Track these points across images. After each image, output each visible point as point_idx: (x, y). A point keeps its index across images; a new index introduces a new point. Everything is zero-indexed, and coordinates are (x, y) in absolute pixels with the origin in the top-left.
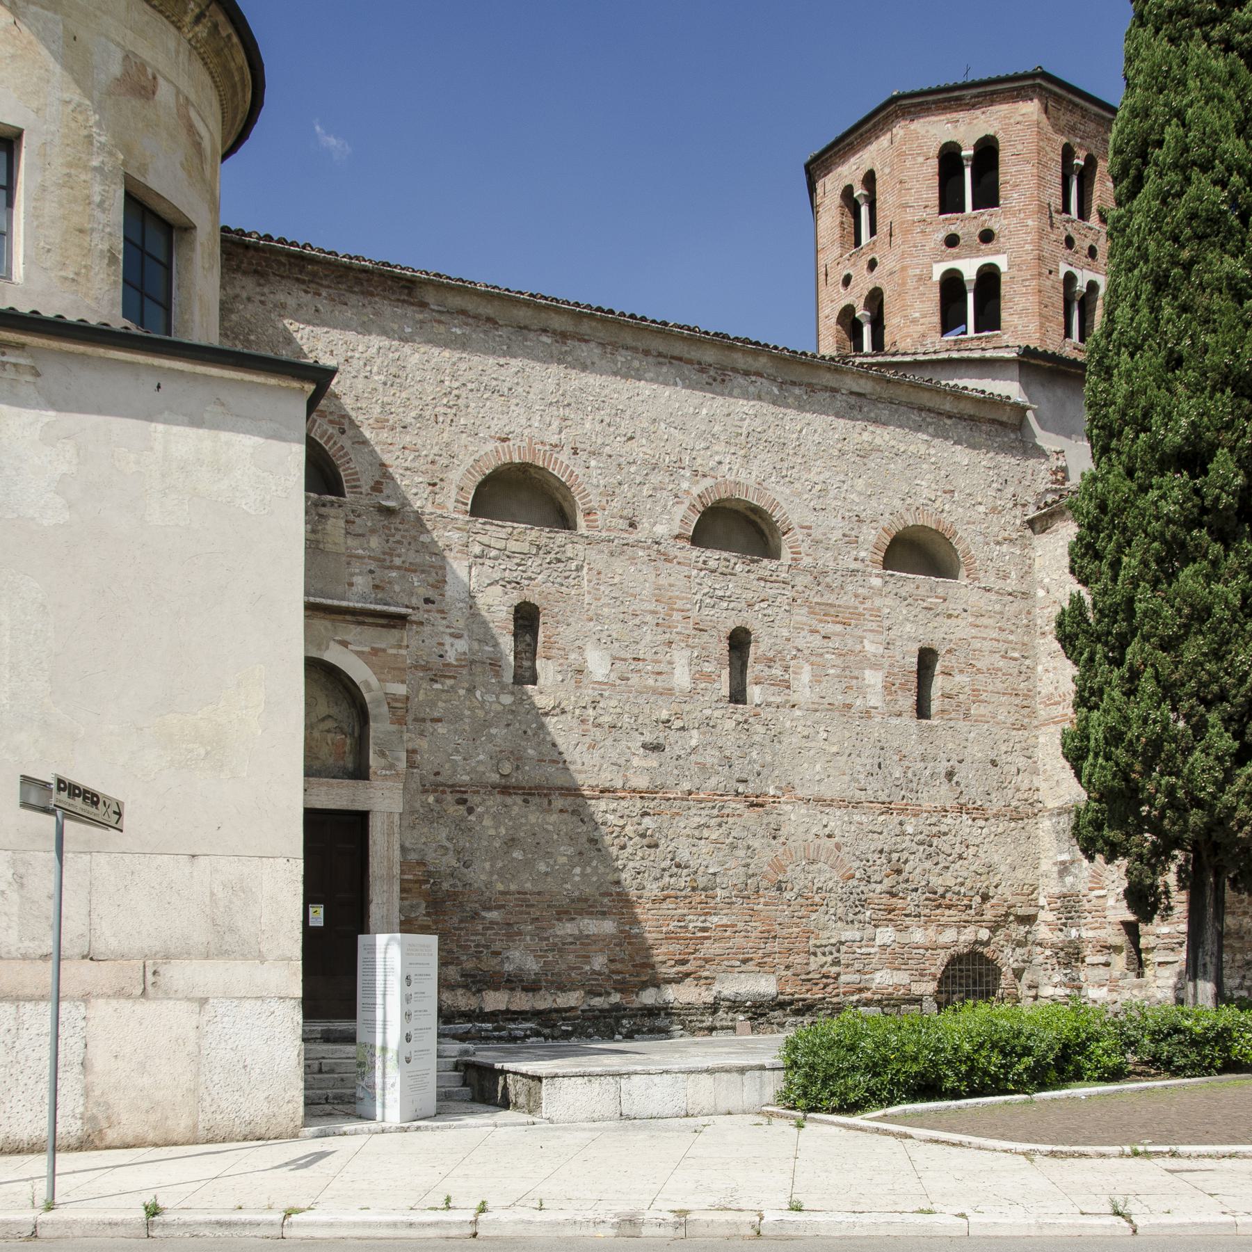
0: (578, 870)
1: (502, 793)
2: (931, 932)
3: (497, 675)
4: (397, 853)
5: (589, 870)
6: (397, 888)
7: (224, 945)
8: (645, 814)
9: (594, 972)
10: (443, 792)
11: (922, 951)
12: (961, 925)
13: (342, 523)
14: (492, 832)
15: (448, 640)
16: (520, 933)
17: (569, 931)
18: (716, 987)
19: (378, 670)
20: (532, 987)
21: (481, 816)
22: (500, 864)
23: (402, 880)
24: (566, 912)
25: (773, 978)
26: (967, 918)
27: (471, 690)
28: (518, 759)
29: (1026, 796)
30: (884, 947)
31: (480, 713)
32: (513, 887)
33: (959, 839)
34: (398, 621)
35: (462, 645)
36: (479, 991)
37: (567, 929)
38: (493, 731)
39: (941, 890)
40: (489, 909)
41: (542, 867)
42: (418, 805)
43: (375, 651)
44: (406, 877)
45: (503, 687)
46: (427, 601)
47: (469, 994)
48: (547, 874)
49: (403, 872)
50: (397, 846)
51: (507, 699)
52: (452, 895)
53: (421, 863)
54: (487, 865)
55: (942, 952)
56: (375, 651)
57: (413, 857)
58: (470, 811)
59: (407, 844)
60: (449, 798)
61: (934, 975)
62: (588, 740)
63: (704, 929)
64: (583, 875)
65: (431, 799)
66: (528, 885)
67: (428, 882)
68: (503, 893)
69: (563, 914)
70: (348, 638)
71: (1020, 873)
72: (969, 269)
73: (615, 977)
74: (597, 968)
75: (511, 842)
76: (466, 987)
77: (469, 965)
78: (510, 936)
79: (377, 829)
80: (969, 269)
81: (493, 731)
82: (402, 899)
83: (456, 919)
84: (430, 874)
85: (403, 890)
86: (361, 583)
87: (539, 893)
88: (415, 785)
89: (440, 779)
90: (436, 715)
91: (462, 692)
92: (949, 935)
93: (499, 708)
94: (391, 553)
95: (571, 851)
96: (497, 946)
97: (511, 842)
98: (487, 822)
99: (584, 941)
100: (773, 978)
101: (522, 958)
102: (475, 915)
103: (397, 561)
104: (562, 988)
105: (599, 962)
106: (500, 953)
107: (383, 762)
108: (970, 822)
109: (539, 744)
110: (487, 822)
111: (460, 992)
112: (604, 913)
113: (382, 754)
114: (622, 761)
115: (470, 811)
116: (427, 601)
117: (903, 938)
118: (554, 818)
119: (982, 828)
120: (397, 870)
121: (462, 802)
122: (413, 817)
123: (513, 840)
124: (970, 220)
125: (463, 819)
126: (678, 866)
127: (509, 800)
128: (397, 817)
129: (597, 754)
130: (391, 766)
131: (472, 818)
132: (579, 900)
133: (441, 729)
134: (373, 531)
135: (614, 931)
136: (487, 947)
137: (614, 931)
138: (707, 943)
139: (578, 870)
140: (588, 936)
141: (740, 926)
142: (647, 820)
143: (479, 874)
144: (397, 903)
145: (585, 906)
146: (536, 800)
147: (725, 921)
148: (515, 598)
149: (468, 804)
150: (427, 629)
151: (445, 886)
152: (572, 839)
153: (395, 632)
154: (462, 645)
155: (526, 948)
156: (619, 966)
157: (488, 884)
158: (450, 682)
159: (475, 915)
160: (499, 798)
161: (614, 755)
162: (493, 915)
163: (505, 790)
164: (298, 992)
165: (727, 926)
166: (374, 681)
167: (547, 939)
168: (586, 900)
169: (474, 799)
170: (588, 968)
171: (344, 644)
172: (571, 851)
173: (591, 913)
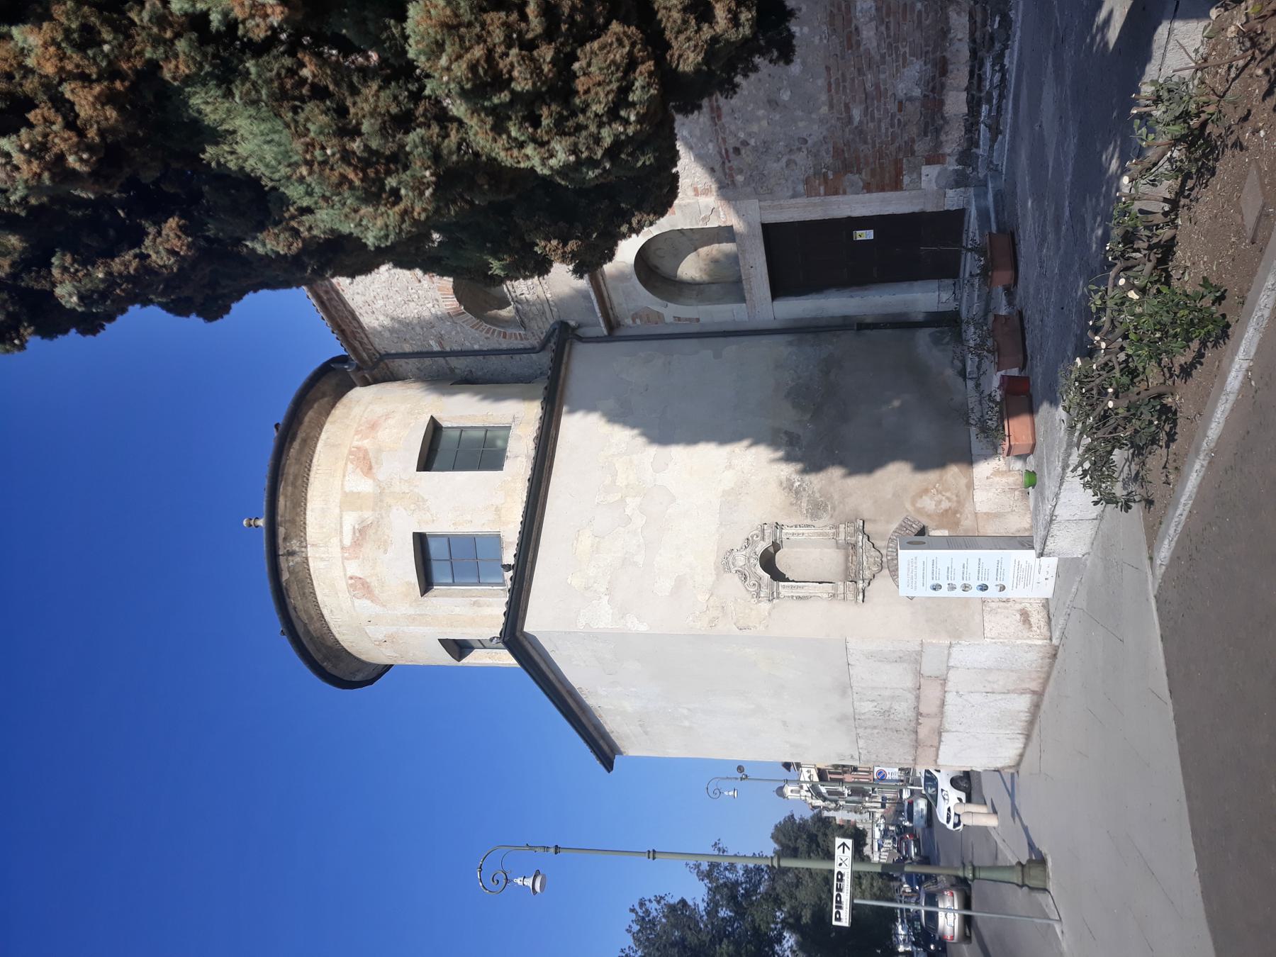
1: (719, 117)
4: (799, 200)
6: (834, 198)
10: (731, 168)
14: (764, 123)
16: (877, 86)
17: (872, 33)
20: (942, 67)
21: (750, 135)
22: (799, 113)
23: (826, 194)
24: (849, 39)
32: (824, 97)
36: (943, 118)
37: (868, 34)
40: (850, 119)
42: (749, 190)
44: (822, 192)
47: (947, 128)
49: (818, 195)
50: (793, 201)
52: (838, 153)
53: (807, 181)
54: (801, 124)
57: (801, 188)
58: (745, 143)
59: (790, 193)
60: (735, 164)
65: (740, 178)
67: (825, 175)
68: (831, 106)
69: (851, 39)
76: (938, 131)
77: (914, 130)
82: (845, 193)
85: (836, 193)
87: (828, 69)
89: (717, 167)
96: (893, 107)
98: (755, 128)
101: (908, 80)
102: (860, 131)
104: (944, 33)
106: (900, 103)
110: (755, 128)
111: (943, 138)
113: (706, 219)
115: (745, 143)
120: (816, 200)
121: (737, 151)
123: (769, 102)
125: (755, 149)
128: (762, 204)
131: (752, 142)
132: (831, 24)
136: (893, 116)
140: (877, 9)
149: (738, 145)
151: (828, 160)
157: (822, 121)
159: (860, 131)
162: (857, 113)
167: (883, 56)
168: (832, 15)
169: (732, 142)
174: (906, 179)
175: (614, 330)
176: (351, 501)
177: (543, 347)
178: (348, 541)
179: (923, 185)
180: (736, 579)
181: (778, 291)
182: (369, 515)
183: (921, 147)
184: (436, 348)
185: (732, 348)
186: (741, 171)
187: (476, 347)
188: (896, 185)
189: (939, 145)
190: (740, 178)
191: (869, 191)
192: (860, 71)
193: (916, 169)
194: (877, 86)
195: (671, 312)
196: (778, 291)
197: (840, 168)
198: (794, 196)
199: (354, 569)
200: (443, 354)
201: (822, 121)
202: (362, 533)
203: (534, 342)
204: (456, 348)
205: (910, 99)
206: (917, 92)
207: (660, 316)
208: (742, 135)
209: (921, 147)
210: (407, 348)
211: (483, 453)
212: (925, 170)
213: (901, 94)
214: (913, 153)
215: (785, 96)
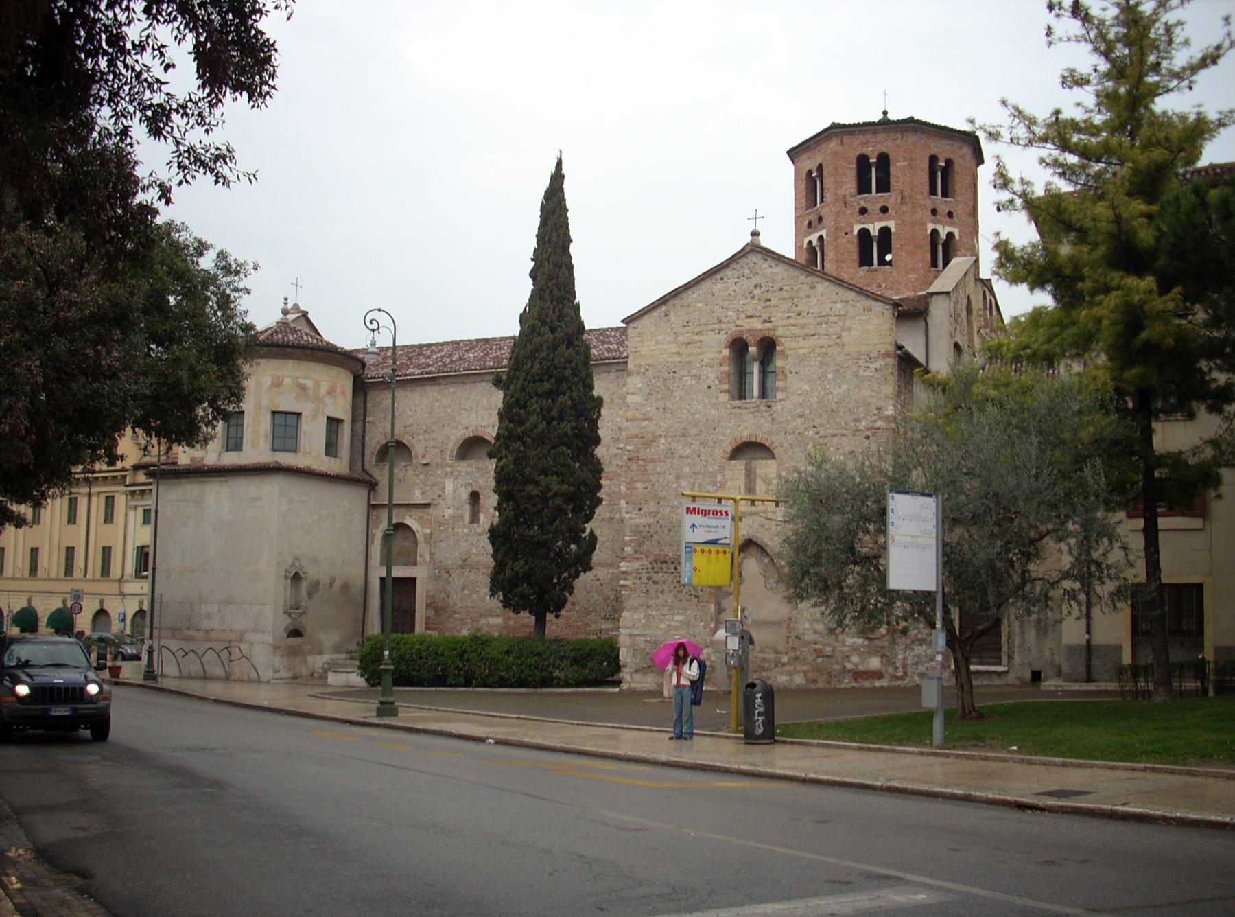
28: (469, 554)
35: (450, 511)
51: (466, 531)
72: (874, 230)
75: (464, 588)
80: (874, 230)
86: (417, 492)
88: (431, 566)
97: (464, 588)
124: (874, 199)
133: (443, 545)
148: (470, 490)
154: (450, 511)
163: (462, 567)
176: (317, 384)
178: (300, 380)
182: (311, 392)
199: (287, 381)
200: (364, 421)
202: (304, 388)
203: (367, 467)
204: (367, 429)
211: (331, 448)
215: (466, 592)
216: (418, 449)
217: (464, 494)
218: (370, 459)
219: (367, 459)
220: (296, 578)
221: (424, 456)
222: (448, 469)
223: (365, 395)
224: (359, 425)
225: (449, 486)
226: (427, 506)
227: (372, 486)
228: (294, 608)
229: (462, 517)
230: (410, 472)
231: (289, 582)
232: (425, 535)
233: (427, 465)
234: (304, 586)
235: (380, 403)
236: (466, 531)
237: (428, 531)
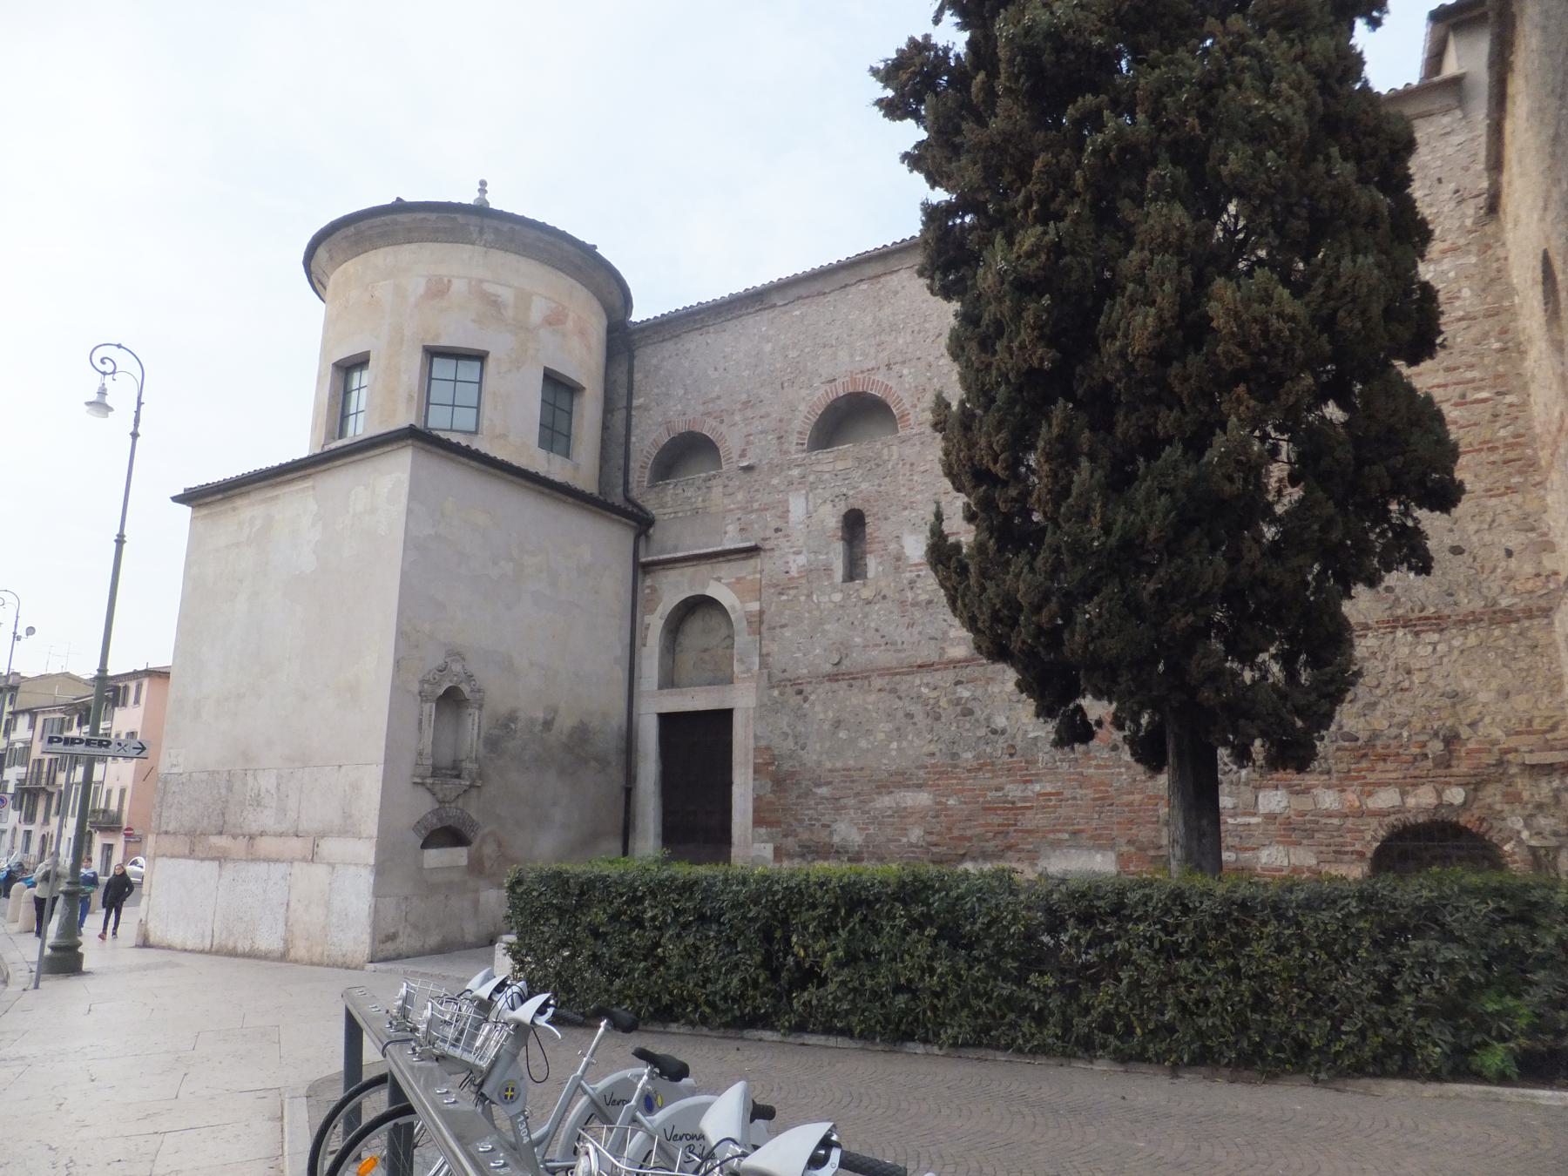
0: (894, 745)
2: (1352, 797)
3: (830, 577)
5: (905, 744)
7: (347, 830)
8: (958, 683)
9: (911, 845)
11: (1336, 821)
12: (1407, 785)
13: (721, 489)
14: (822, 716)
15: (792, 557)
16: (844, 807)
18: (1042, 864)
19: (741, 595)
21: (813, 704)
22: (828, 744)
24: (884, 786)
25: (1112, 856)
26: (1417, 773)
27: (809, 596)
28: (844, 648)
29: (1530, 585)
30: (1271, 817)
31: (816, 613)
32: (839, 765)
33: (1391, 663)
34: (753, 551)
35: (802, 560)
37: (885, 801)
38: (827, 627)
39: (1363, 736)
40: (819, 785)
41: (863, 744)
42: (765, 700)
43: (739, 580)
45: (834, 588)
46: (777, 530)
48: (868, 750)
51: (837, 597)
53: (768, 748)
54: (818, 746)
55: (1374, 822)
56: (739, 580)
57: (763, 743)
58: (805, 700)
60: (790, 690)
61: (1361, 855)
62: (906, 620)
63: (1024, 799)
64: (899, 749)
65: (776, 693)
66: (851, 762)
68: (831, 771)
69: (883, 787)
70: (721, 574)
71: (1521, 702)
73: (934, 849)
74: (913, 839)
75: (837, 724)
76: (803, 856)
77: (805, 836)
78: (837, 810)
79: (738, 720)
81: (827, 627)
83: (794, 795)
84: (774, 757)
85: (755, 772)
88: (764, 682)
89: (787, 675)
90: (783, 621)
91: (803, 598)
92: (1386, 799)
93: (831, 606)
94: (752, 500)
95: (888, 727)
96: (826, 819)
97: (837, 724)
98: (818, 708)
99: (901, 813)
100: (1112, 856)
101: (847, 832)
103: (756, 505)
105: (915, 834)
107: (743, 668)
108: (1409, 638)
109: (864, 631)
112: (919, 786)
113: (741, 661)
114: (939, 636)
115: (805, 700)
116: (777, 530)
117: (1304, 803)
118: (872, 698)
119: (1435, 645)
121: (800, 692)
122: (767, 709)
123: (839, 722)
125: (800, 707)
126: (994, 732)
127: (835, 686)
129: (915, 630)
130: (749, 670)
131: (806, 705)
132: (897, 773)
133: (787, 633)
134: (740, 488)
135: (929, 802)
137: (929, 802)
138: (1029, 814)
139: (894, 745)
141: (1067, 793)
142: (959, 689)
143: (810, 758)
144: (751, 782)
145: (900, 778)
146: (859, 682)
147: (1049, 789)
148: (843, 508)
150: (777, 553)
152: (890, 716)
153: (752, 562)
155: (852, 820)
156: (934, 838)
157: (819, 763)
158: (792, 592)
160: (827, 685)
161: (931, 631)
162: (824, 791)
163: (833, 678)
164: (372, 862)
165: (1051, 794)
166: (737, 603)
169: (808, 689)
170: (904, 840)
171: (719, 579)
172: (888, 727)
173: (908, 786)
174: (762, 831)
175: (642, 569)
177: (628, 499)
179: (756, 845)
180: (440, 662)
181: (666, 719)
183: (790, 843)
184: (636, 403)
185: (621, 674)
186: (782, 694)
187: (633, 439)
188: (758, 821)
189: (791, 856)
190: (776, 693)
191: (755, 800)
192: (858, 794)
193: (771, 839)
194: (844, 807)
195: (655, 623)
196: (666, 719)
197: (778, 777)
198: (756, 737)
200: (629, 408)
201: (819, 763)
203: (634, 493)
204: (634, 421)
205: (831, 833)
206: (836, 839)
207: (652, 611)
208: (812, 697)
209: (790, 843)
210: (638, 377)
212: (769, 848)
213: (835, 826)
214: (785, 836)
215: (842, 735)
216: (731, 441)
217: (831, 519)
218: (640, 475)
219: (634, 477)
220: (451, 701)
221: (743, 455)
222: (796, 472)
223: (632, 358)
224: (620, 416)
225: (797, 507)
226: (753, 551)
227: (641, 523)
228: (441, 773)
229: (828, 570)
230: (717, 491)
231: (429, 708)
232: (748, 615)
233: (749, 469)
234: (473, 727)
235: (657, 368)
236: (837, 597)
237: (754, 606)
